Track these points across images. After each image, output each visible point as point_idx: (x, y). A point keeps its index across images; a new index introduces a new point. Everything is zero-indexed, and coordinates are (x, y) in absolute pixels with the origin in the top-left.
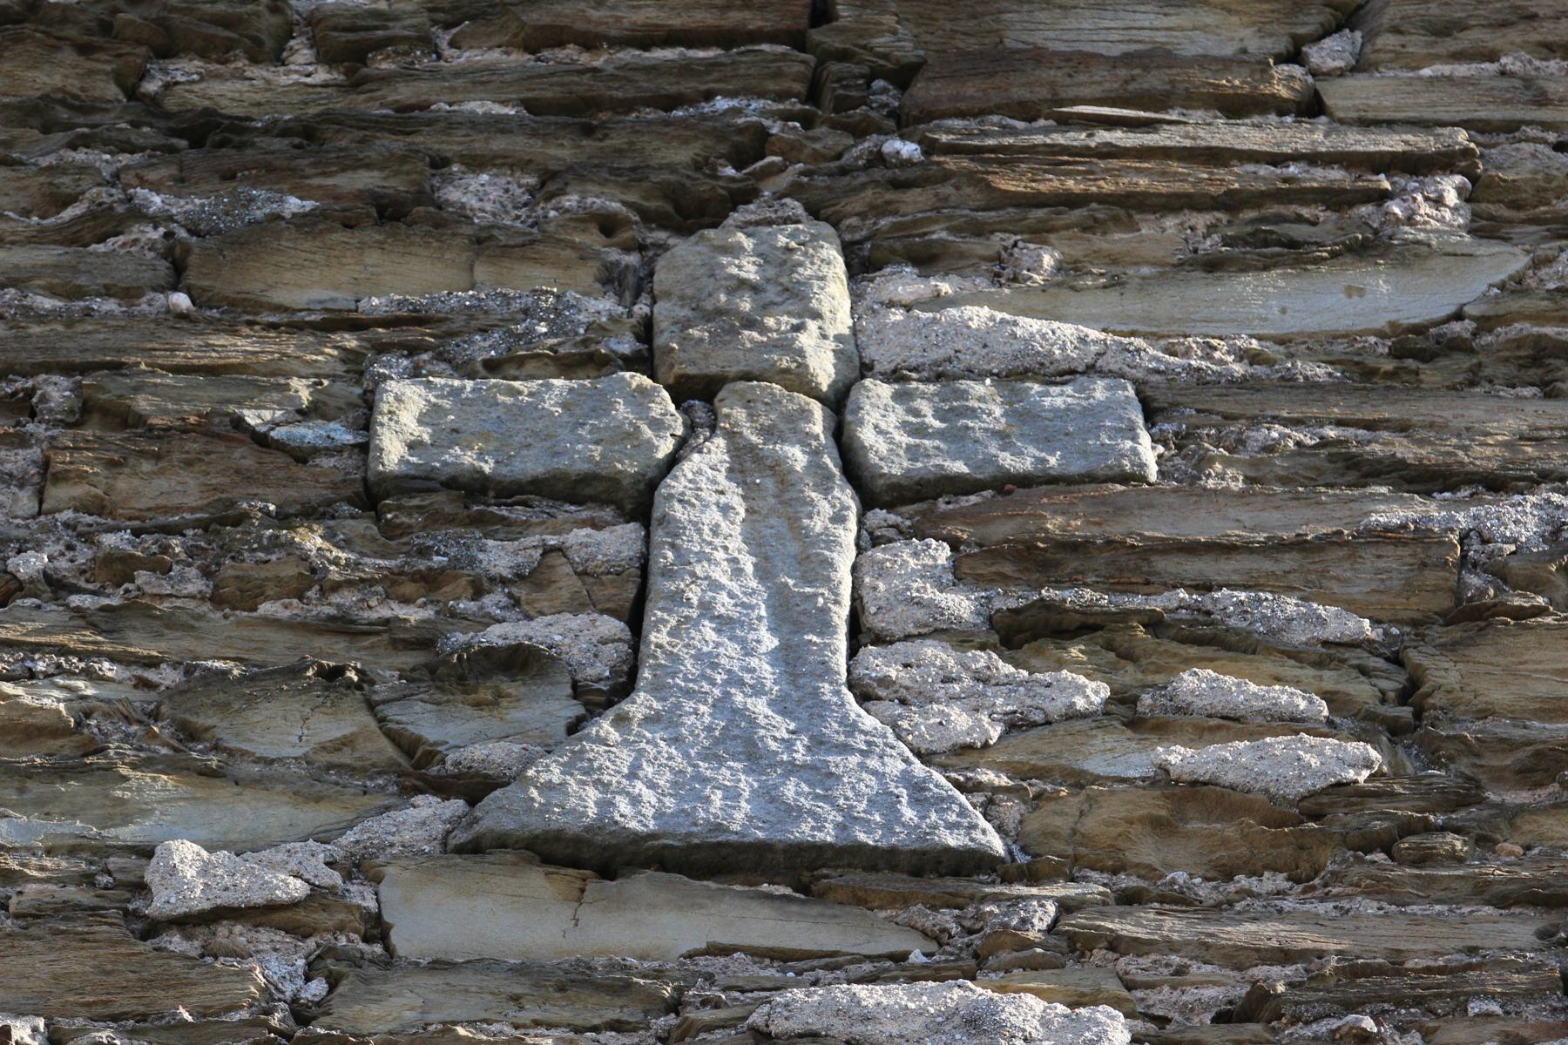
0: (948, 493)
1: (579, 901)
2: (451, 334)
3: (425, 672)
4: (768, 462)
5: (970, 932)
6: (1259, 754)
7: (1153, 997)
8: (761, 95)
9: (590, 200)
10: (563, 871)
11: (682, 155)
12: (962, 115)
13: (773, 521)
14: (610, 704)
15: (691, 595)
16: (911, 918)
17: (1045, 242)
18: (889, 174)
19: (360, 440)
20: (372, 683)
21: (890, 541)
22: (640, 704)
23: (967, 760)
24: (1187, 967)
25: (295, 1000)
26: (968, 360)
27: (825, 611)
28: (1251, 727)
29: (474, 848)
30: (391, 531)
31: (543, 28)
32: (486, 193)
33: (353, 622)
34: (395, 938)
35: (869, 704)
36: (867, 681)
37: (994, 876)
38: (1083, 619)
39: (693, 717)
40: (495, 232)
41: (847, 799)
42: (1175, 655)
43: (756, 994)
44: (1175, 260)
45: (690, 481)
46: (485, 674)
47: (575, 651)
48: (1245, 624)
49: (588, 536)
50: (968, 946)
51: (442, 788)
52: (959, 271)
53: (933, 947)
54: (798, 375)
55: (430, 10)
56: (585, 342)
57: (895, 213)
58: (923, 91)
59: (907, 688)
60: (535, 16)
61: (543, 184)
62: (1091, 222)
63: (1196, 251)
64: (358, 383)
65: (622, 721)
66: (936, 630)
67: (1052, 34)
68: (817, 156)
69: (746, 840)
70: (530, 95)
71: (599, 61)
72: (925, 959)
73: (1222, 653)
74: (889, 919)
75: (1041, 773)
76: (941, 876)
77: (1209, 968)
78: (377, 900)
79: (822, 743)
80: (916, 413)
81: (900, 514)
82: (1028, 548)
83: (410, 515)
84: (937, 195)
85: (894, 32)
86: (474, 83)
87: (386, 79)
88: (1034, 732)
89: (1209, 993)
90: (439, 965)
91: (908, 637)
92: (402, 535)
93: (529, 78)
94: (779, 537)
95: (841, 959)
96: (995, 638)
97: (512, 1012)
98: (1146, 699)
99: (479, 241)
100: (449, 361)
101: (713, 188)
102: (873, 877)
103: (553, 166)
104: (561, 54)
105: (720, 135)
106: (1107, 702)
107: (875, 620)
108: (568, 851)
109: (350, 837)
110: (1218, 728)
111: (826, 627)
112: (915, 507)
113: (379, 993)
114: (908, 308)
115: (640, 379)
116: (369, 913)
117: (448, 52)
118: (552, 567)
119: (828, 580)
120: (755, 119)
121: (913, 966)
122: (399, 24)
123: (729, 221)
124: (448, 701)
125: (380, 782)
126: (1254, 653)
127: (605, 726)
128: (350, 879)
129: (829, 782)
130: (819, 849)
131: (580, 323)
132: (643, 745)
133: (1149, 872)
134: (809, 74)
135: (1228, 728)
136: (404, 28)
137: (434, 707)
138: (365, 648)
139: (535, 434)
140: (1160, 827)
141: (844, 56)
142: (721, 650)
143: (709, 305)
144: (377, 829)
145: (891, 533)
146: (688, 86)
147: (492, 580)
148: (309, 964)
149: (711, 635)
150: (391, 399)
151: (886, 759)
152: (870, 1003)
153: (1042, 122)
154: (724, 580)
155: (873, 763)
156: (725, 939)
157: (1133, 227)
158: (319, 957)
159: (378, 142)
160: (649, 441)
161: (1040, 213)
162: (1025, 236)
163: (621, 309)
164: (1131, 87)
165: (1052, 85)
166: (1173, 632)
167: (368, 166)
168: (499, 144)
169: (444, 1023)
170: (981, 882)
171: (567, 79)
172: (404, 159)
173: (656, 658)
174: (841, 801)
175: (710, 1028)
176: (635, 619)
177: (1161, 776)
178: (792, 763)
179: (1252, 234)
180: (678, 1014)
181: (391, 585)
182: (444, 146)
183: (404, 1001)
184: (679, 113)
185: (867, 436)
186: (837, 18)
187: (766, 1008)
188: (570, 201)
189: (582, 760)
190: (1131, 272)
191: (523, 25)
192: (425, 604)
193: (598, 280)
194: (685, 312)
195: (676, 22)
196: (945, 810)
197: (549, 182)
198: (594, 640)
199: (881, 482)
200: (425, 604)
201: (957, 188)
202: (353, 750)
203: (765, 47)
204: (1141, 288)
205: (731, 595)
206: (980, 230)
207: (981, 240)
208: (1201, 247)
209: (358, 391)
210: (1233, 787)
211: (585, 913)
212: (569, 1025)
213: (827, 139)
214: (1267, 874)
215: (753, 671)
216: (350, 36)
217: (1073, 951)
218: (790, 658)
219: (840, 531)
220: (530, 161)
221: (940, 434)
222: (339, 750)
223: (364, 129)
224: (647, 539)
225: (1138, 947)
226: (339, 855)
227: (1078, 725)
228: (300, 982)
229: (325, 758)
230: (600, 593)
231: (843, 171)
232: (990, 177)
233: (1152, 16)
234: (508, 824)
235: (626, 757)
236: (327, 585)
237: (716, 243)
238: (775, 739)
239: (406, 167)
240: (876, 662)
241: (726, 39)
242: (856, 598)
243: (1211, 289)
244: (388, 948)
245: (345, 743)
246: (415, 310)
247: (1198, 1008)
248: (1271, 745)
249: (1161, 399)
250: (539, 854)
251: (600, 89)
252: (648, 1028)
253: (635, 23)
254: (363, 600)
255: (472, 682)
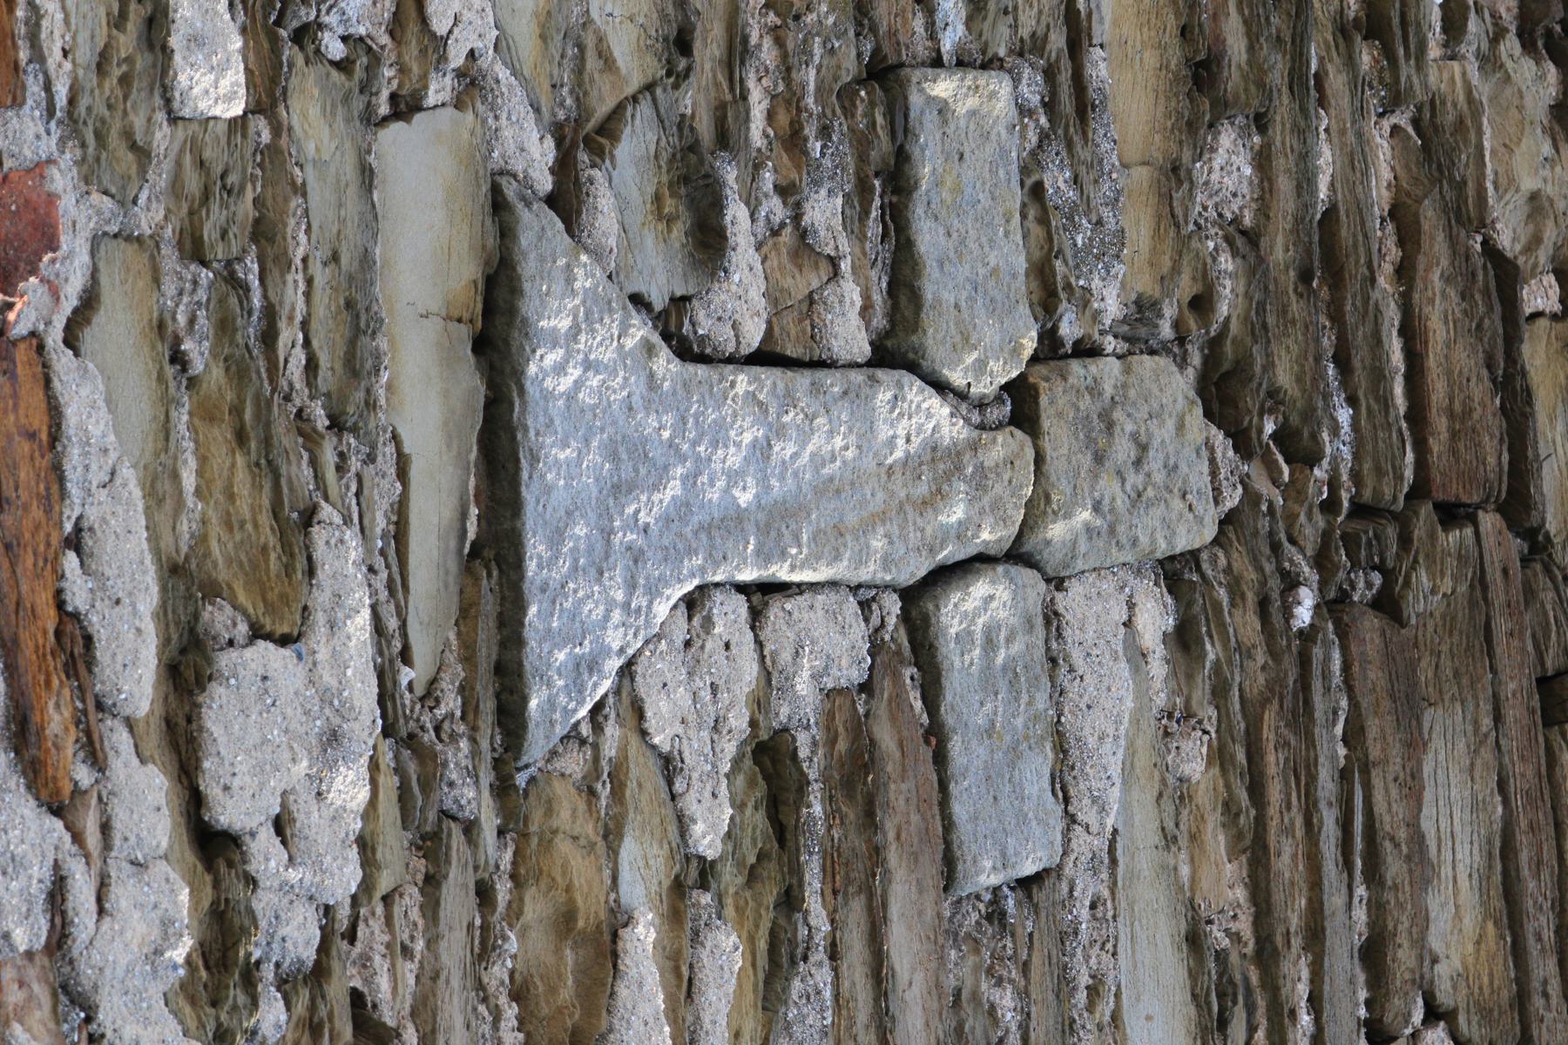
0: (923, 677)
1: (448, 318)
2: (1070, 145)
3: (691, 141)
4: (945, 487)
5: (437, 729)
6: (651, 1020)
7: (377, 925)
8: (1356, 456)
9: (1228, 283)
10: (479, 299)
11: (1284, 377)
12: (1346, 667)
13: (880, 496)
14: (666, 337)
15: (791, 414)
16: (449, 666)
17: (1209, 763)
18: (1275, 595)
19: (945, 58)
20: (676, 86)
21: (867, 620)
22: (665, 363)
23: (628, 714)
24: (412, 959)
25: (320, 26)
26: (1073, 689)
27: (783, 555)
28: (682, 1011)
29: (498, 205)
30: (846, 96)
31: (1418, 222)
32: (1230, 173)
33: (743, 63)
34: (397, 127)
35: (683, 608)
36: (708, 604)
37: (500, 750)
38: (791, 827)
39: (656, 424)
40: (1186, 186)
41: (575, 591)
42: (757, 926)
43: (355, 508)
44: (1198, 900)
45: (919, 406)
46: (692, 203)
47: (723, 297)
48: (795, 997)
49: (853, 303)
50: (422, 728)
51: (564, 166)
52: (1174, 673)
53: (420, 690)
54: (1045, 513)
55: (1432, 102)
56: (1068, 287)
57: (1233, 605)
58: (1370, 626)
59: (702, 647)
60: (1430, 213)
61: (1243, 233)
62: (1234, 809)
63: (1210, 922)
64: (1011, 52)
65: (649, 349)
66: (769, 673)
67: (1442, 757)
68: (1291, 518)
69: (523, 488)
70: (1342, 213)
71: (1384, 282)
72: (404, 682)
73: (761, 976)
74: (447, 643)
75: (618, 793)
76: (498, 696)
77: (412, 981)
78: (436, 107)
79: (636, 562)
80: (1009, 640)
81: (896, 628)
82: (865, 765)
83: (865, 115)
84: (1254, 646)
85: (1433, 592)
86: (1352, 154)
87: (1350, 62)
88: (662, 783)
89: (384, 983)
90: (367, 176)
91: (759, 644)
92: (843, 107)
93: (1360, 209)
94: (863, 503)
95: (400, 595)
96: (764, 735)
97: (319, 256)
98: (706, 898)
99: (1175, 169)
100: (1040, 146)
101: (1249, 412)
102: (492, 624)
103: (1264, 242)
104: (1391, 244)
105: (1309, 414)
106: (702, 859)
107: (776, 610)
108: (501, 303)
109: (503, 73)
110: (679, 976)
111: (764, 556)
112: (906, 643)
113: (333, 114)
114: (1128, 624)
115: (1029, 345)
116: (421, 99)
117: (1386, 124)
118: (817, 268)
119: (818, 558)
120: (1328, 450)
121: (396, 673)
122: (1413, 71)
123: (1214, 430)
124: (660, 167)
125: (569, 102)
126: (764, 1008)
127: (640, 330)
128: (458, 76)
129: (593, 572)
130: (518, 564)
131: (1089, 280)
132: (622, 373)
133: (515, 912)
134: (1382, 505)
135: (679, 987)
136: (1409, 77)
137: (652, 151)
138: (715, 76)
139: (963, 242)
140: (565, 921)
141: (1405, 540)
142: (732, 450)
143: (1118, 415)
144: (514, 102)
145: (875, 620)
146: (1361, 378)
147: (798, 205)
148: (361, 39)
149: (747, 438)
150: (992, 87)
151: (622, 630)
152: (350, 626)
153: (1342, 751)
154: (810, 448)
155: (617, 616)
156: (415, 473)
157: (1232, 855)
158: (370, 49)
159: (1279, 57)
160: (961, 361)
161: (1241, 756)
162: (1215, 743)
163: (1108, 322)
164: (1388, 844)
165: (1385, 761)
166: (782, 922)
167: (1251, 48)
168: (1285, 185)
169: (304, 184)
170: (492, 737)
171: (1361, 250)
172: (1261, 85)
173: (720, 382)
174: (571, 585)
175: (314, 463)
176: (764, 357)
177: (622, 918)
178: (612, 532)
179: (1231, 982)
180: (328, 428)
181: (787, 100)
182: (1279, 128)
183: (326, 141)
184: (1331, 370)
185: (980, 588)
186: (1446, 530)
187: (338, 520)
188: (1226, 262)
189: (601, 312)
190: (1183, 855)
191: (1419, 202)
192: (767, 136)
193: (1140, 296)
194: (1108, 390)
195: (1432, 362)
196: (569, 695)
197: (1246, 239)
198: (736, 316)
199: (931, 607)
200: (767, 136)
201: (1263, 668)
202: (601, 71)
203: (1410, 456)
204: (1164, 867)
205: (795, 456)
206: (1219, 693)
207: (1208, 696)
208: (1215, 928)
209: (1002, 52)
210: (612, 995)
211: (434, 326)
212: (309, 314)
213: (1311, 529)
214: (521, 1036)
215: (712, 484)
216: (1396, 21)
217: (423, 838)
218: (732, 522)
219: (786, 565)
220: (1268, 217)
221: (988, 665)
222: (600, 56)
223: (1293, 42)
224: (854, 365)
225: (431, 907)
226: (484, 63)
227: (673, 830)
228: (341, 31)
229: (590, 41)
230: (789, 320)
231: (1276, 548)
232: (1276, 702)
233: (1468, 861)
234: (526, 239)
235: (608, 355)
236: (781, 33)
237: (1188, 418)
238: (637, 511)
239: (1252, 88)
240: (730, 613)
241: (1417, 415)
242: (800, 588)
243: (1168, 941)
244: (385, 120)
245: (608, 62)
246: (1094, 107)
247: (367, 973)
248: (661, 1032)
249: (1039, 896)
250: (496, 272)
251: (1352, 288)
252: (312, 398)
253: (1428, 319)
254: (767, 70)
255: (683, 191)
